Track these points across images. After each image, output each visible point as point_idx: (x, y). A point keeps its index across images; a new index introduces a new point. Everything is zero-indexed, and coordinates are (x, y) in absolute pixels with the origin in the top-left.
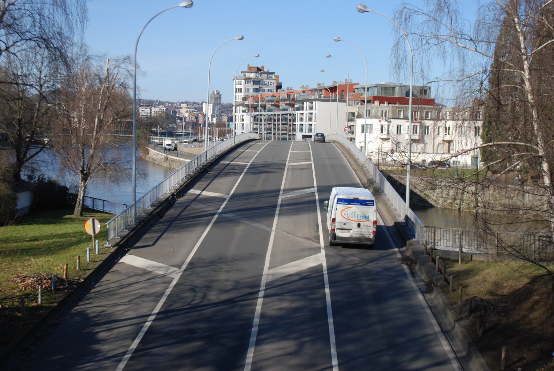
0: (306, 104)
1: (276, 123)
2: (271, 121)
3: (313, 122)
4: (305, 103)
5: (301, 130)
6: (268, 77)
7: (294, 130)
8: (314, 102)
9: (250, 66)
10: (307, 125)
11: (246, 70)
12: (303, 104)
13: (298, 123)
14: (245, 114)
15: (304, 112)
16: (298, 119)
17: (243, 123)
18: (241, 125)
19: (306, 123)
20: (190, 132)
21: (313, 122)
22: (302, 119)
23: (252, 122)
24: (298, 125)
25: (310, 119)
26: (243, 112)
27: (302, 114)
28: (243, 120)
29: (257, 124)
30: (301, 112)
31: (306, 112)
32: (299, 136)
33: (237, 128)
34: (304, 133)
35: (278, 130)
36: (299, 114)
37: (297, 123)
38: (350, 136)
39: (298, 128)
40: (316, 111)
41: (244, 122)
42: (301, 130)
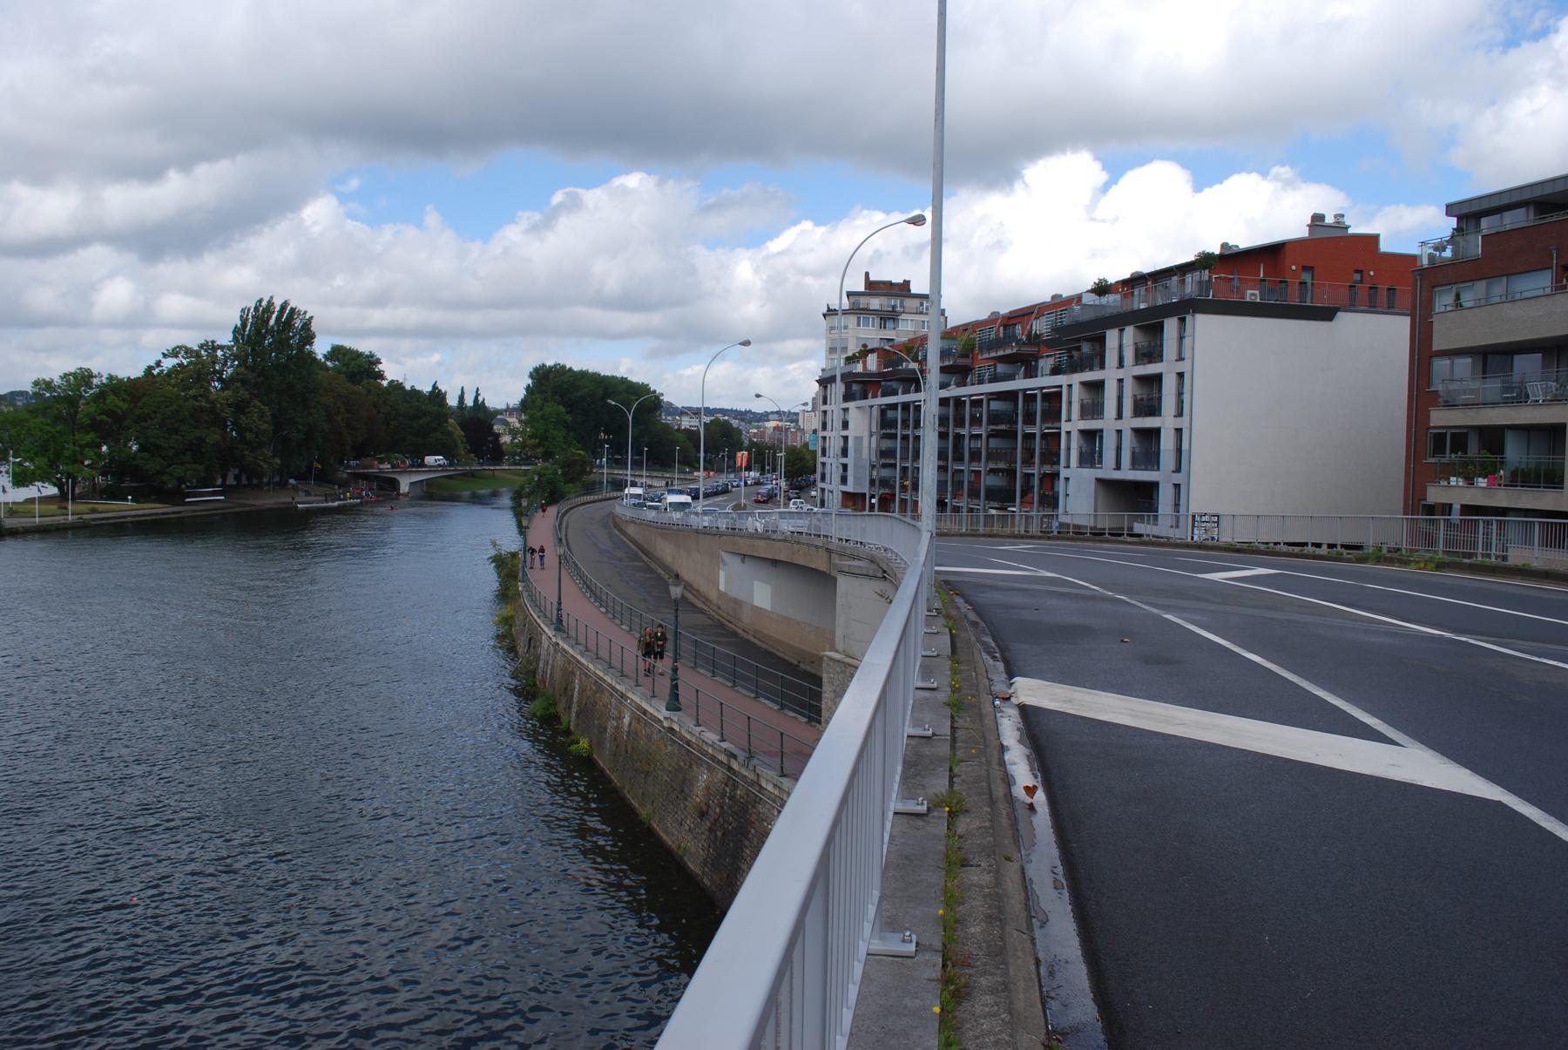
0: (1122, 341)
3: (1183, 423)
4: (1112, 336)
5: (1090, 457)
7: (1052, 456)
8: (1170, 325)
9: (872, 278)
11: (862, 289)
12: (1101, 340)
13: (1072, 425)
14: (851, 405)
17: (845, 433)
20: (629, 472)
21: (1183, 423)
23: (874, 429)
24: (1075, 436)
25: (1148, 407)
26: (848, 397)
27: (1096, 387)
28: (845, 425)
29: (894, 436)
34: (1107, 471)
35: (975, 456)
39: (1072, 447)
41: (850, 433)
42: (1090, 457)
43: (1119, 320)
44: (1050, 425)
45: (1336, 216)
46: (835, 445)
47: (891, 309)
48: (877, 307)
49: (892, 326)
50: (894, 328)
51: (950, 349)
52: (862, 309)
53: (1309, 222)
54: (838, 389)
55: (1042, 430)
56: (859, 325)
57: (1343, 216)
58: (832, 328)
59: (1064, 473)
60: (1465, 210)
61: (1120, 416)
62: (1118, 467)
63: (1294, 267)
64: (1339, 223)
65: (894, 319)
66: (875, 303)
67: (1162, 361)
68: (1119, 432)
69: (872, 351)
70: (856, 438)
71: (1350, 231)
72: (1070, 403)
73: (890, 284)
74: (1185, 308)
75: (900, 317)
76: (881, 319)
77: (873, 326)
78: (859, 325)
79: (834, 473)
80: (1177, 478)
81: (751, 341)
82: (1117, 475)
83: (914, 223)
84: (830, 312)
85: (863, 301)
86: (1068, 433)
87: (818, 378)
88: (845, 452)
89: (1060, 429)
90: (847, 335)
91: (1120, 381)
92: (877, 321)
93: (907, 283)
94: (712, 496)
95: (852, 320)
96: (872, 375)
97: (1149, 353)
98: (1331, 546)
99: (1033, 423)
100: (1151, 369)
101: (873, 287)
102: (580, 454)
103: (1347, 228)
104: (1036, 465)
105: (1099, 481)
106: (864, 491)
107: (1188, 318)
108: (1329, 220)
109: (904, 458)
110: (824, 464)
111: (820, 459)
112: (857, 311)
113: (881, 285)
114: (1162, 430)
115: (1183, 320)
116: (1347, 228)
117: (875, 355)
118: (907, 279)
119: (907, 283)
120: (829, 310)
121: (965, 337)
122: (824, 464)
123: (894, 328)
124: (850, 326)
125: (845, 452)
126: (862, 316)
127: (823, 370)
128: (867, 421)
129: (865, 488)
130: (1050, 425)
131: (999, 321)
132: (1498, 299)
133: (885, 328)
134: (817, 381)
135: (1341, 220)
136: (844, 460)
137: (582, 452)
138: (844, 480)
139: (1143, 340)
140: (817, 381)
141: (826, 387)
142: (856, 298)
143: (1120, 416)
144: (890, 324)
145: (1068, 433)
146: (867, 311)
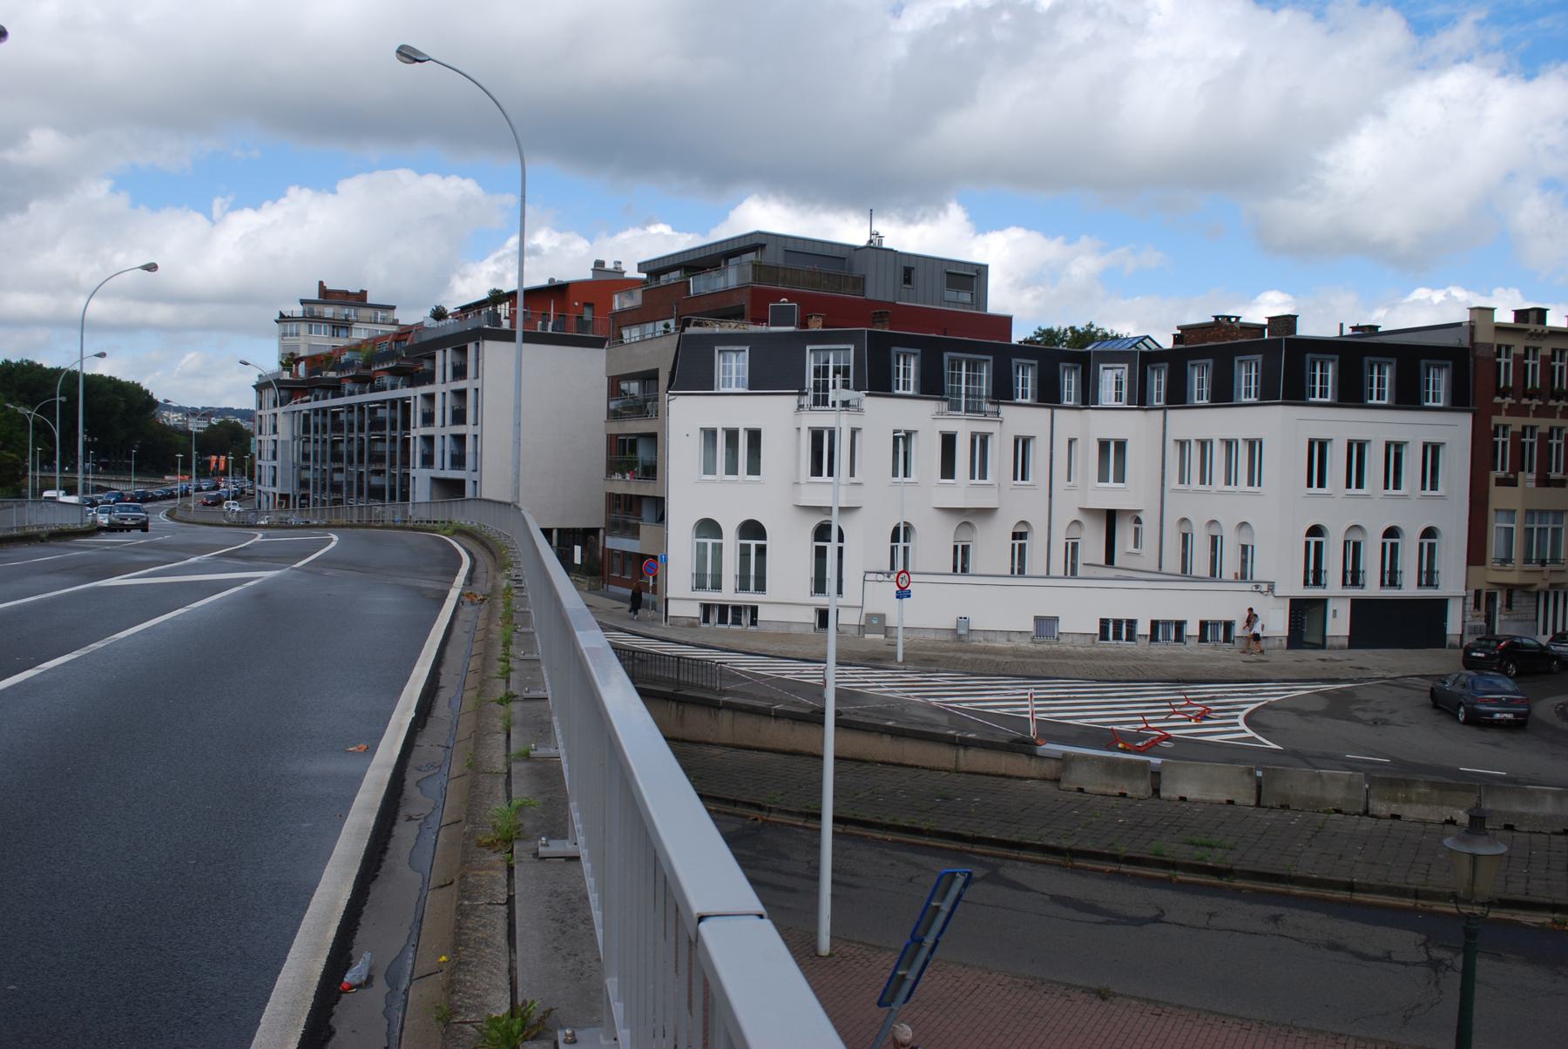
0: (444, 360)
1: (354, 435)
2: (333, 430)
3: (467, 429)
4: (439, 354)
5: (428, 461)
6: (376, 318)
8: (471, 347)
9: (329, 287)
10: (448, 439)
12: (433, 358)
13: (417, 431)
15: (437, 388)
16: (416, 417)
18: (271, 447)
19: (442, 430)
21: (467, 429)
22: (428, 419)
24: (418, 439)
25: (459, 417)
27: (430, 398)
30: (427, 389)
31: (442, 388)
32: (421, 479)
33: (264, 455)
34: (437, 472)
36: (419, 398)
37: (413, 433)
38: (626, 485)
39: (417, 450)
40: (477, 384)
42: (428, 461)
43: (442, 342)
44: (336, 435)
45: (615, 262)
46: (268, 448)
47: (344, 318)
48: (330, 316)
49: (345, 334)
50: (347, 337)
51: (353, 361)
52: (315, 317)
53: (593, 267)
54: (270, 395)
55: (401, 435)
56: (310, 332)
57: (620, 263)
58: (285, 335)
59: (412, 473)
60: (652, 268)
61: (444, 425)
62: (443, 469)
63: (576, 304)
64: (616, 268)
65: (347, 328)
66: (329, 311)
67: (465, 378)
68: (443, 437)
69: (301, 359)
70: (283, 441)
71: (626, 275)
72: (415, 412)
73: (347, 293)
74: (480, 335)
75: (353, 326)
76: (334, 327)
77: (325, 334)
78: (310, 332)
79: (267, 475)
80: (475, 476)
81: (107, 353)
82: (442, 475)
83: (148, 270)
84: (283, 318)
85: (317, 309)
86: (415, 438)
87: (255, 384)
88: (274, 457)
89: (409, 434)
90: (297, 342)
91: (444, 394)
92: (329, 329)
93: (363, 294)
94: (164, 499)
95: (304, 327)
96: (303, 382)
97: (460, 372)
98: (428, 522)
99: (325, 433)
100: (460, 385)
101: (327, 295)
102: (12, 458)
103: (623, 273)
104: (397, 466)
105: (433, 479)
106: (287, 493)
107: (481, 343)
108: (609, 265)
109: (393, 464)
110: (260, 466)
111: (258, 462)
112: (311, 319)
113: (337, 294)
114: (467, 437)
115: (477, 344)
116: (623, 273)
117: (303, 363)
118: (365, 289)
119: (363, 294)
120: (282, 316)
121: (369, 348)
122: (260, 466)
123: (347, 337)
124: (302, 333)
125: (274, 457)
126: (314, 324)
127: (260, 376)
128: (290, 426)
129: (288, 491)
130: (336, 435)
131: (391, 337)
132: (650, 336)
133: (338, 336)
134: (254, 386)
135: (618, 266)
136: (274, 463)
137: (14, 455)
138: (274, 484)
139: (458, 359)
140: (254, 386)
141: (261, 392)
142: (311, 306)
143: (444, 425)
144: (343, 332)
145: (415, 438)
146: (320, 319)
